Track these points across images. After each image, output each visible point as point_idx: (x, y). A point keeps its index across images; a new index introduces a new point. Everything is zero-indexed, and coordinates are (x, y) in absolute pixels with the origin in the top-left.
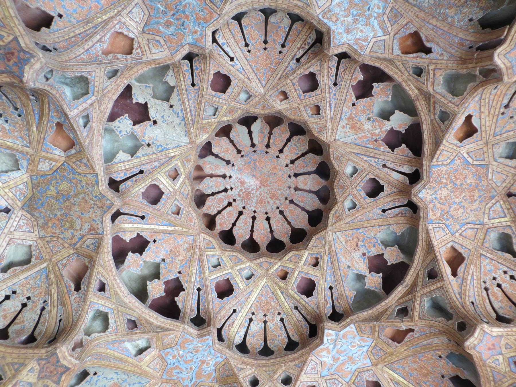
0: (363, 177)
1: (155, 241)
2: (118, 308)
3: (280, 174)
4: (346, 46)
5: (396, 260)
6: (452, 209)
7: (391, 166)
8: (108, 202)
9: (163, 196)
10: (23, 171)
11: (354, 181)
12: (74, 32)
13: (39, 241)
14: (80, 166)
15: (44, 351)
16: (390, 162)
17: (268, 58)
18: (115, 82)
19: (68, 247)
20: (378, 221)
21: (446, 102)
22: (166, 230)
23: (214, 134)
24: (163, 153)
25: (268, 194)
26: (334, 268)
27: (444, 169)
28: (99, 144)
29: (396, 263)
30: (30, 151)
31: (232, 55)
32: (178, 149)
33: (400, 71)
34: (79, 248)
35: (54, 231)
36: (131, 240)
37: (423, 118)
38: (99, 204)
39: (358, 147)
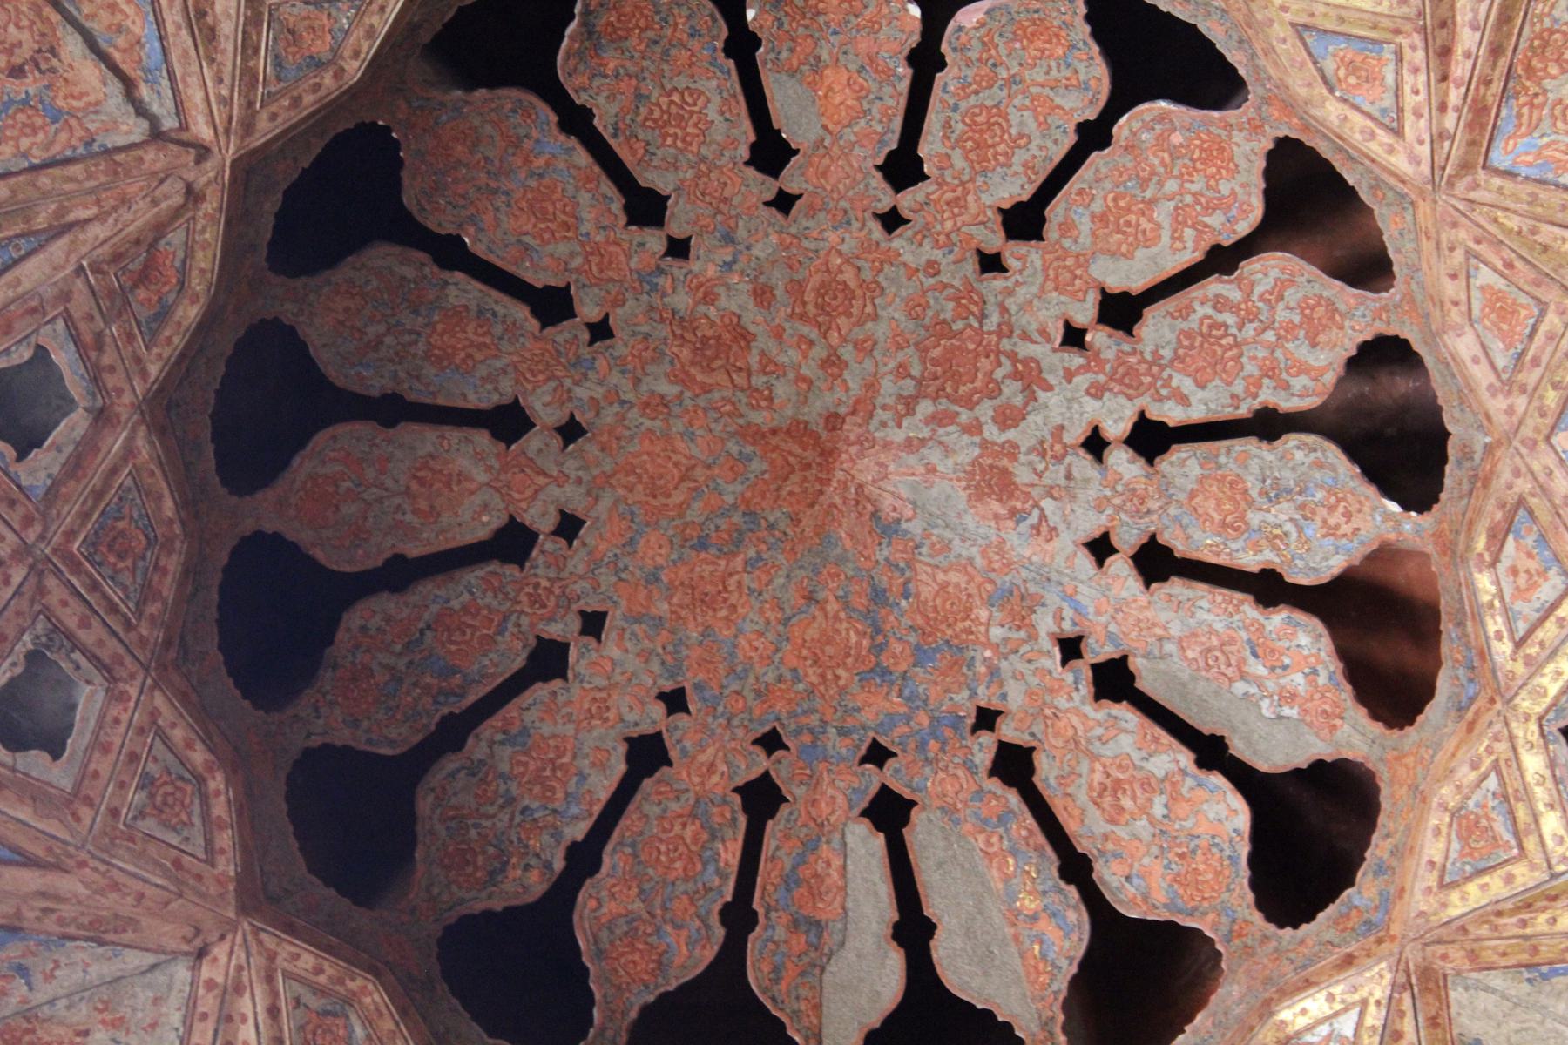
3: (654, 549)
32: (1546, 953)
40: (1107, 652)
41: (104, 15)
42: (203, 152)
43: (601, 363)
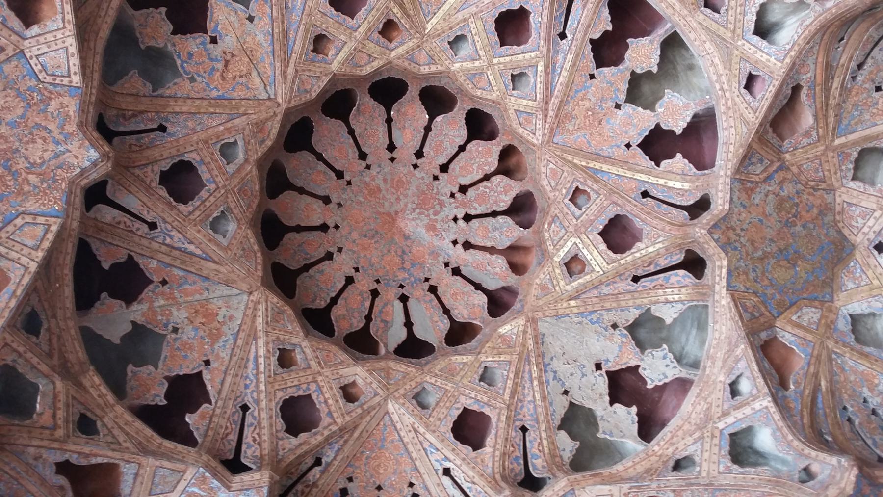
0: (201, 208)
1: (628, 146)
2: (733, 38)
3: (355, 235)
4: (234, 486)
5: (148, 14)
6: (20, 112)
7: (138, 224)
8: (716, 236)
9: (602, 227)
10: (844, 311)
11: (218, 203)
14: (754, 307)
16: (139, 233)
17: (374, 469)
18: (677, 449)
19: (793, 165)
20: (177, 109)
21: (29, 355)
22: (605, 162)
23: (486, 330)
24: (590, 308)
25: (384, 197)
26: (283, 22)
27: (31, 205)
28: (714, 342)
29: (148, 8)
31: (446, 480)
33: (120, 427)
34: (775, 160)
35: (811, 198)
36: (671, 156)
37: (71, 324)
38: (731, 234)
39: (205, 273)
40: (455, 266)
41: (263, 69)
42: (279, 105)
43: (348, 190)
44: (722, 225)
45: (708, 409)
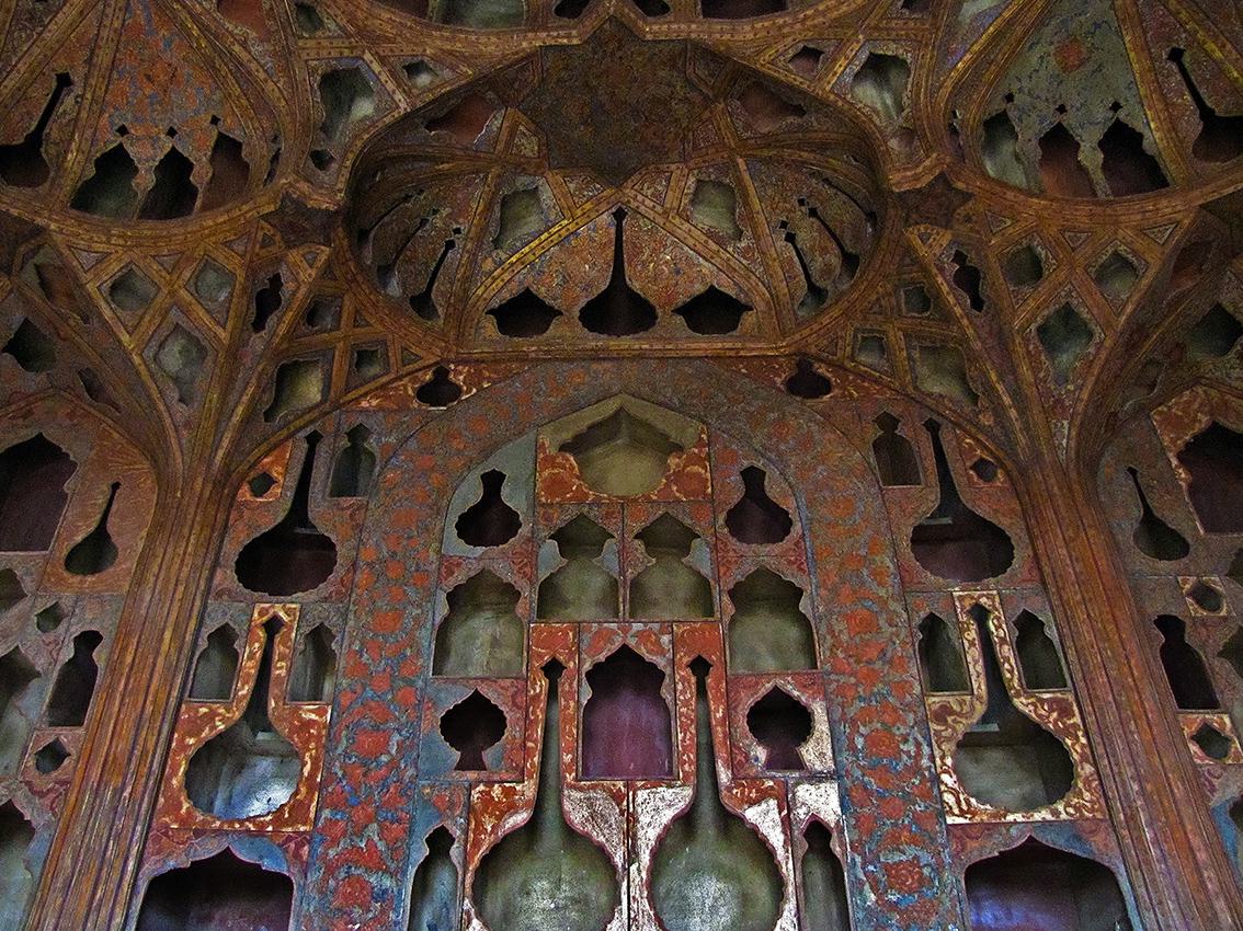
12: (238, 97)
13: (691, 164)
15: (892, 212)
30: (495, 170)
44: (624, 33)
45: (387, 38)
